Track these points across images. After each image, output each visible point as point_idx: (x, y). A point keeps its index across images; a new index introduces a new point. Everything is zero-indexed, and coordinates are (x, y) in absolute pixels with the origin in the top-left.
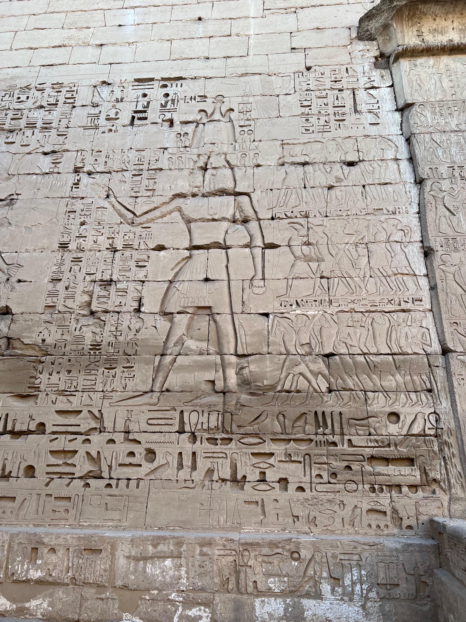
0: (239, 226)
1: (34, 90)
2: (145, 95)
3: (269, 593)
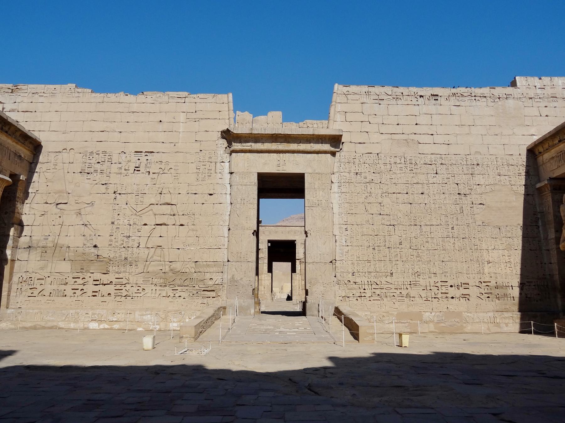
0: (172, 217)
1: (95, 154)
2: (139, 159)
3: (174, 322)
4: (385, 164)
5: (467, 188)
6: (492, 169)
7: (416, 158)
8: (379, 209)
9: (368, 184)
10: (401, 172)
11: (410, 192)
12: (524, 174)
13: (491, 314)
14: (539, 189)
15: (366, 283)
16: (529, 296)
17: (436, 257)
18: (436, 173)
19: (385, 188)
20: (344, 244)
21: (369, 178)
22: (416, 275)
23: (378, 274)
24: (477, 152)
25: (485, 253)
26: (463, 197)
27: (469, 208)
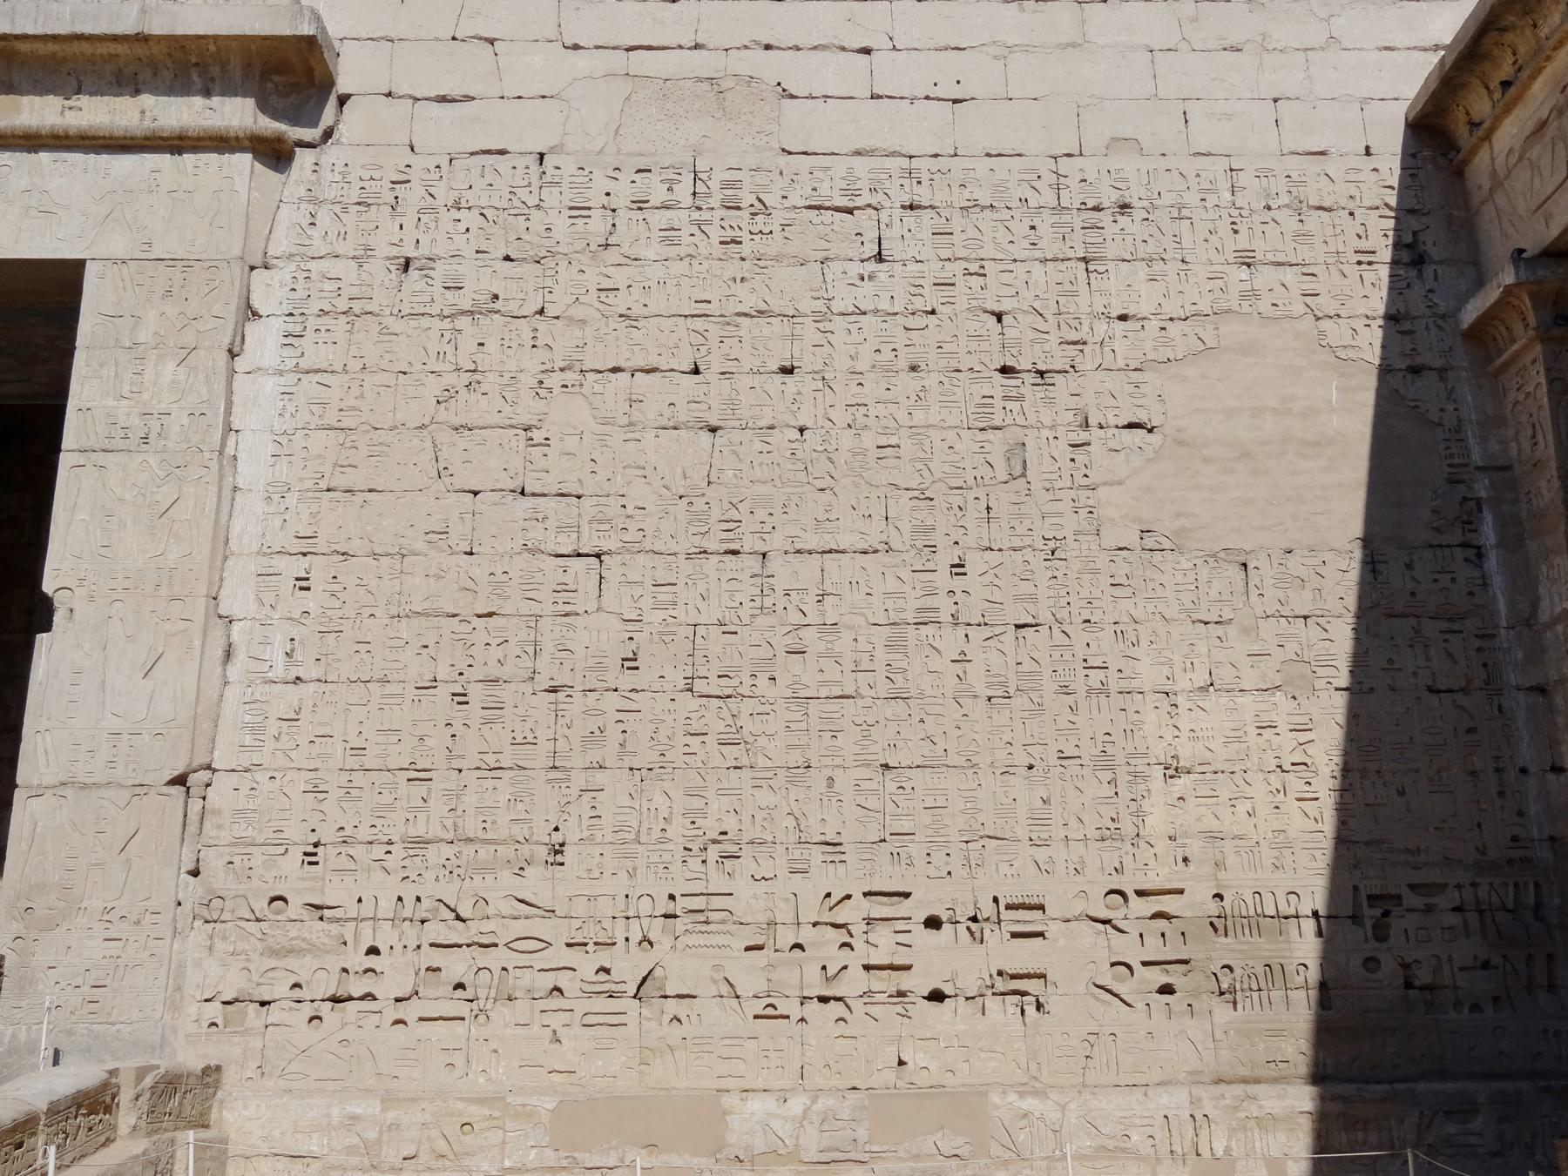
4: (579, 210)
5: (1054, 339)
6: (1202, 228)
7: (760, 178)
8: (516, 462)
9: (463, 322)
10: (673, 251)
11: (714, 363)
12: (1386, 254)
13: (1174, 1101)
14: (1480, 336)
15: (387, 906)
16: (1424, 976)
17: (848, 742)
18: (879, 257)
19: (564, 341)
20: (279, 671)
21: (479, 281)
22: (713, 853)
23: (468, 850)
24: (1117, 143)
25: (1152, 717)
26: (1027, 390)
27: (1062, 450)
